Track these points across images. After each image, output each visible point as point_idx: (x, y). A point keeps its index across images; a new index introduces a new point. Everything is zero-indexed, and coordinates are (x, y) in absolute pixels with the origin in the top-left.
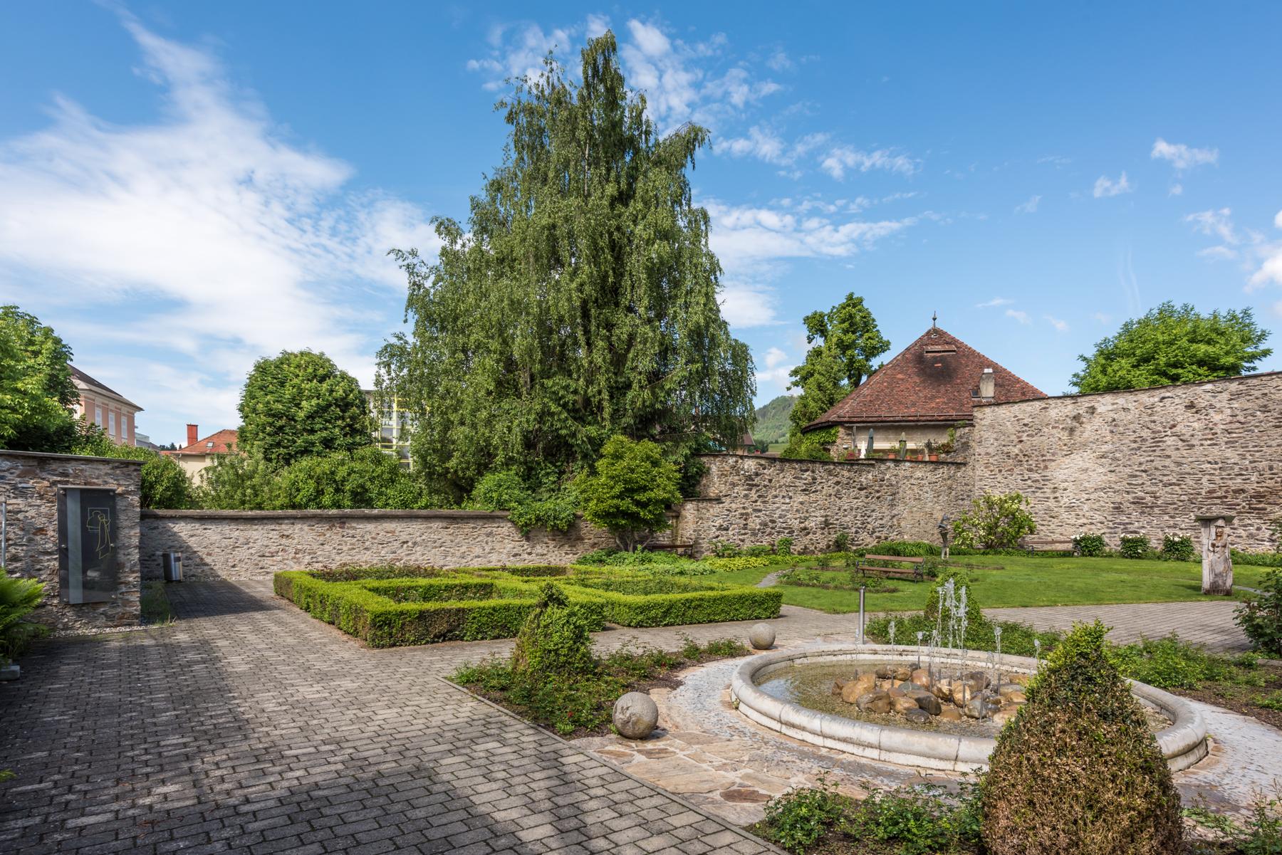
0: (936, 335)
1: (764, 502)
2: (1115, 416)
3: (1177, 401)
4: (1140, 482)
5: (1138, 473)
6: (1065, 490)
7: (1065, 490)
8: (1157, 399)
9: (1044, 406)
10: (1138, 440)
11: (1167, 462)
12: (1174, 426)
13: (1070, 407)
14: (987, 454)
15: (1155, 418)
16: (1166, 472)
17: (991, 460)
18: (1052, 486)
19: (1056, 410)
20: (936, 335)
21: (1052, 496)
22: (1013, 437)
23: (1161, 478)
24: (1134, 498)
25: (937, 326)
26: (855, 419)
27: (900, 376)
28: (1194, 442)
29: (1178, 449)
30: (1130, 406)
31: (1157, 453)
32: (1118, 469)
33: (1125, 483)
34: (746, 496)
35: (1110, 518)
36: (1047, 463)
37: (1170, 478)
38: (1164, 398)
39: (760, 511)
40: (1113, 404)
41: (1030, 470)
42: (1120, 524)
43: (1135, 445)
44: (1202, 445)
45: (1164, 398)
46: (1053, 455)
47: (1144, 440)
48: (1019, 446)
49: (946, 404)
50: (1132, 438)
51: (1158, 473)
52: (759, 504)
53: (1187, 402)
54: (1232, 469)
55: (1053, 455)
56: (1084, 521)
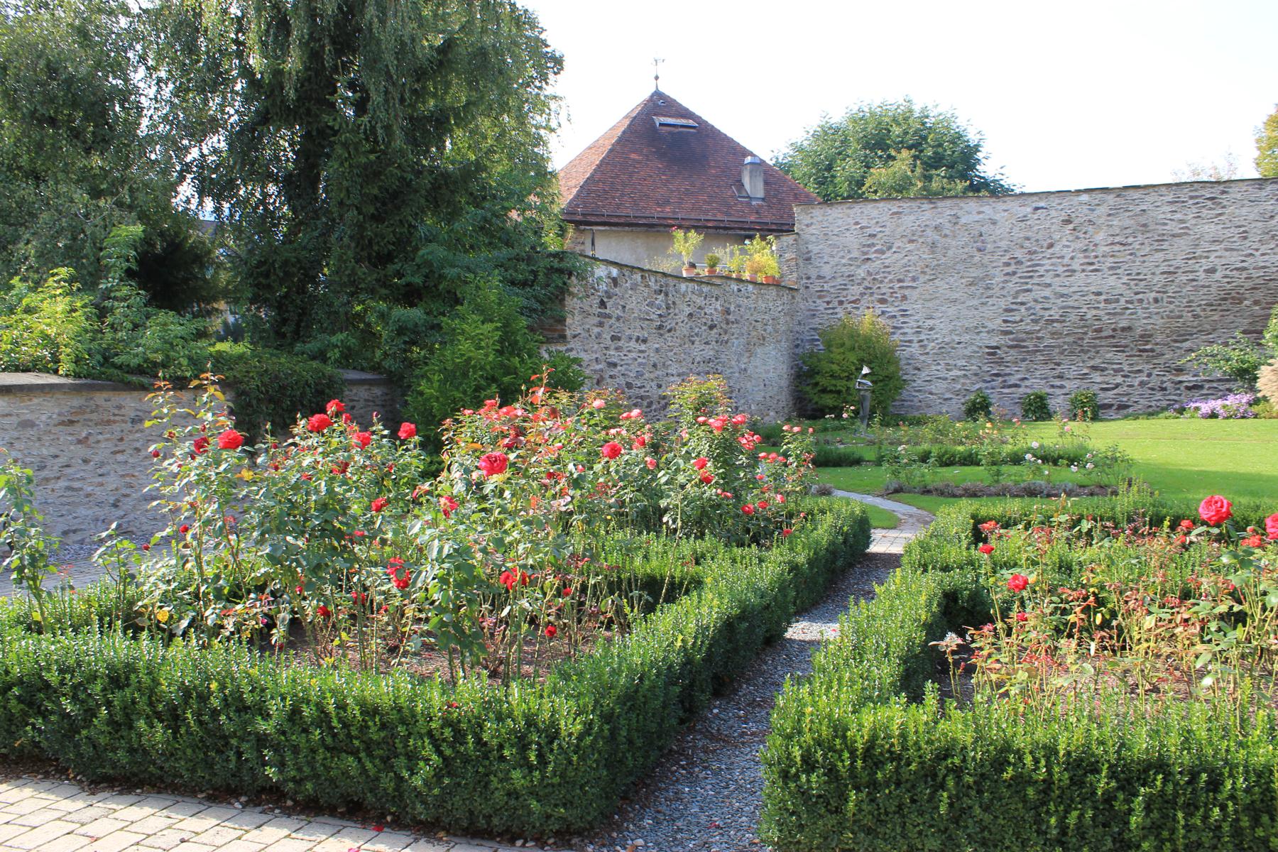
0: (659, 104)
1: (617, 349)
2: (983, 230)
3: (1053, 213)
4: (1018, 318)
5: (1014, 307)
6: (931, 329)
7: (931, 329)
8: (1029, 210)
9: (895, 210)
10: (1013, 261)
11: (1047, 292)
12: (1051, 246)
13: (928, 214)
14: (819, 277)
15: (1030, 234)
16: (1046, 306)
17: (826, 287)
18: (915, 324)
19: (912, 218)
20: (659, 104)
21: (915, 339)
22: (855, 254)
23: (1042, 312)
24: (1012, 340)
25: (662, 89)
26: (593, 219)
27: (633, 156)
28: (1076, 266)
29: (1058, 275)
30: (997, 217)
31: (1036, 280)
32: (991, 301)
33: (999, 321)
34: (599, 336)
35: (985, 368)
36: (907, 292)
37: (1052, 313)
38: (1037, 209)
39: (615, 365)
40: (979, 213)
41: (883, 301)
42: (997, 375)
43: (1010, 269)
44: (1083, 271)
45: (1037, 209)
46: (914, 279)
47: (1019, 263)
48: (867, 266)
49: (709, 203)
50: (1005, 259)
51: (1040, 306)
52: (614, 355)
53: (1064, 216)
54: (1117, 301)
55: (914, 279)
56: (956, 373)
